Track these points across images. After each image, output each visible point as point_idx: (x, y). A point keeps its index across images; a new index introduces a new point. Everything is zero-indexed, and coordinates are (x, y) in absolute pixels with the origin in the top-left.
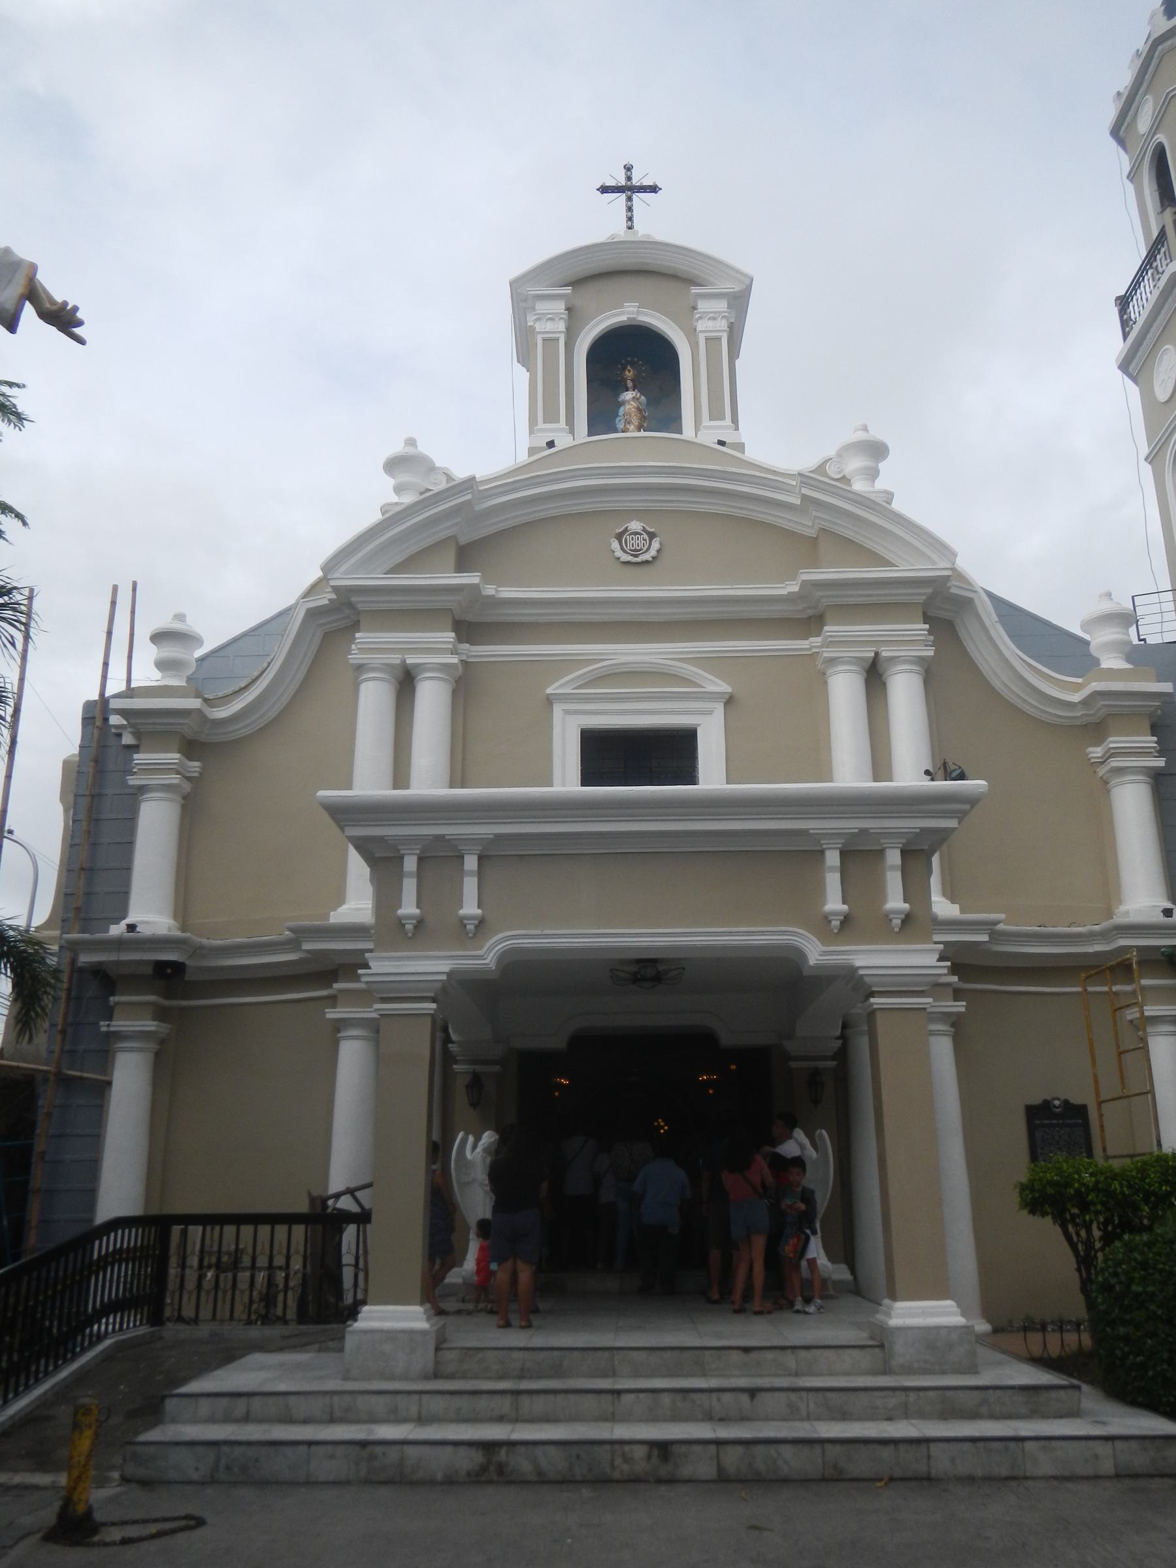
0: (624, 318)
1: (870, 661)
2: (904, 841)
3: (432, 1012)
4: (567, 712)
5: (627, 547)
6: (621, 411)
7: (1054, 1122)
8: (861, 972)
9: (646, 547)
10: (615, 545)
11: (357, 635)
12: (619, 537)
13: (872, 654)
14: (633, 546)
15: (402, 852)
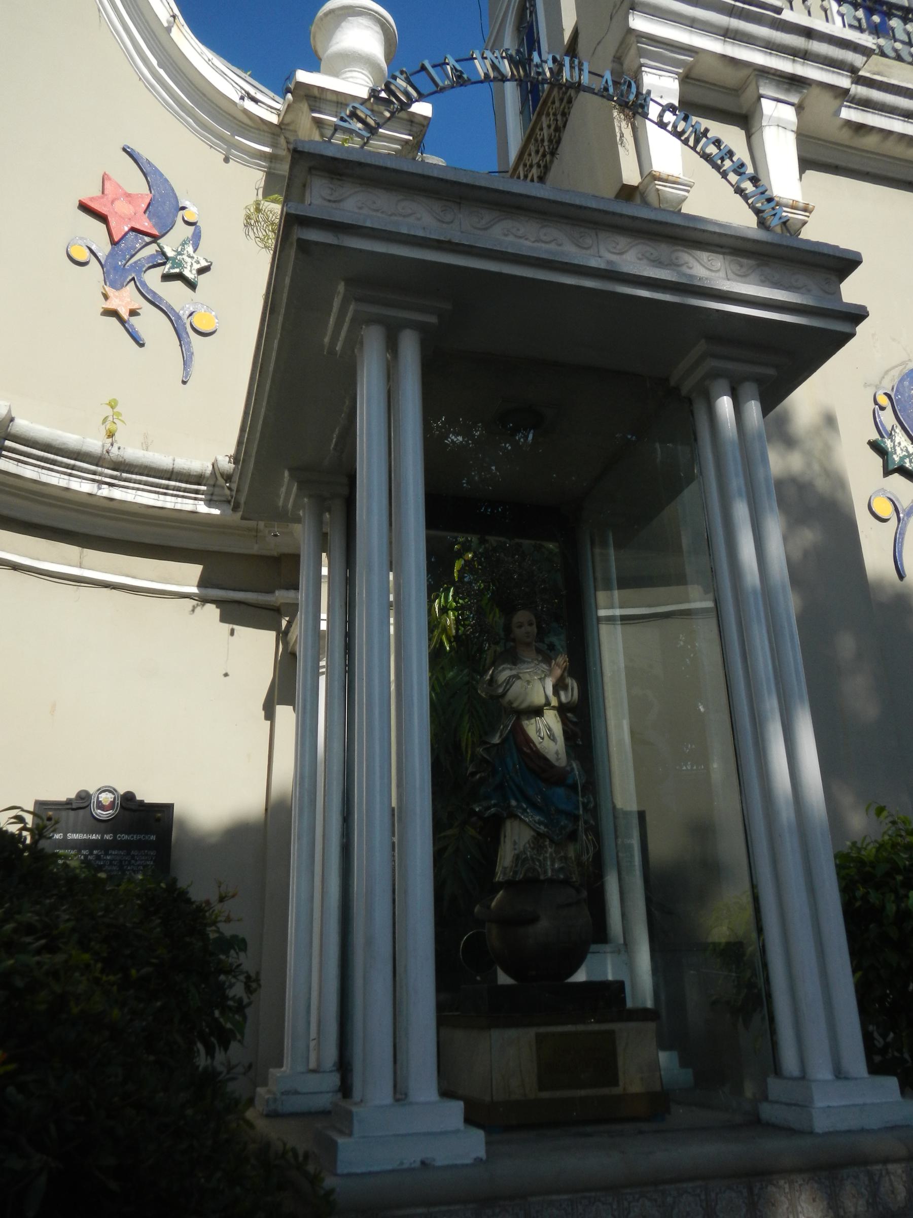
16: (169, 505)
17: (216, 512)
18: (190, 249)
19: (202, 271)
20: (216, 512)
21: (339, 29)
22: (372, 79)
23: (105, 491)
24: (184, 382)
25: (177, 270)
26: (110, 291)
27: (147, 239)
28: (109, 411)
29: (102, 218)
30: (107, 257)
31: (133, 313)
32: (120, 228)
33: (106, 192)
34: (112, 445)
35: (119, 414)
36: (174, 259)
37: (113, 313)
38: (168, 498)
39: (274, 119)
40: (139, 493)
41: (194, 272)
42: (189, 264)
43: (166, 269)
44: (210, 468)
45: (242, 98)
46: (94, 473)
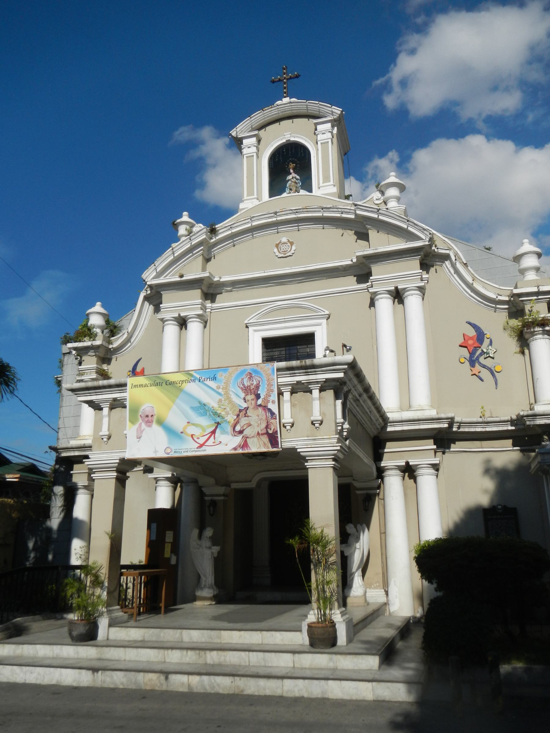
0: (284, 141)
1: (394, 291)
2: (320, 385)
3: (115, 477)
4: (255, 331)
5: (281, 250)
6: (288, 185)
7: (499, 517)
8: (299, 450)
9: (289, 249)
10: (276, 250)
11: (161, 305)
12: (277, 246)
13: (393, 288)
14: (283, 250)
15: (102, 406)
16: (501, 429)
17: (513, 428)
18: (490, 347)
19: (494, 353)
20: (513, 428)
21: (522, 259)
22: (535, 271)
23: (484, 430)
24: (496, 389)
25: (488, 355)
26: (472, 368)
27: (478, 348)
28: (482, 410)
29: (466, 347)
30: (469, 358)
31: (479, 372)
32: (471, 349)
33: (465, 339)
34: (484, 418)
35: (484, 411)
36: (486, 352)
37: (475, 374)
38: (500, 427)
39: (507, 299)
40: (493, 428)
41: (493, 354)
42: (491, 352)
43: (485, 356)
44: (510, 418)
45: (497, 297)
46: (481, 426)
